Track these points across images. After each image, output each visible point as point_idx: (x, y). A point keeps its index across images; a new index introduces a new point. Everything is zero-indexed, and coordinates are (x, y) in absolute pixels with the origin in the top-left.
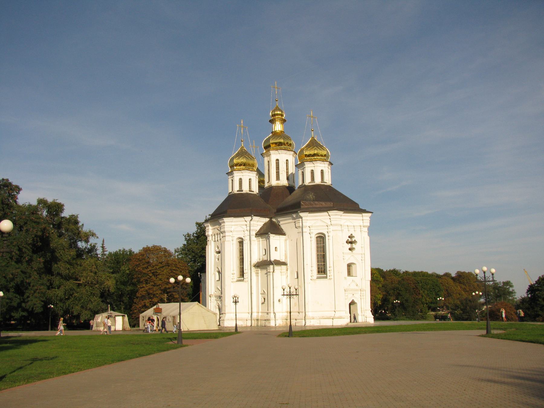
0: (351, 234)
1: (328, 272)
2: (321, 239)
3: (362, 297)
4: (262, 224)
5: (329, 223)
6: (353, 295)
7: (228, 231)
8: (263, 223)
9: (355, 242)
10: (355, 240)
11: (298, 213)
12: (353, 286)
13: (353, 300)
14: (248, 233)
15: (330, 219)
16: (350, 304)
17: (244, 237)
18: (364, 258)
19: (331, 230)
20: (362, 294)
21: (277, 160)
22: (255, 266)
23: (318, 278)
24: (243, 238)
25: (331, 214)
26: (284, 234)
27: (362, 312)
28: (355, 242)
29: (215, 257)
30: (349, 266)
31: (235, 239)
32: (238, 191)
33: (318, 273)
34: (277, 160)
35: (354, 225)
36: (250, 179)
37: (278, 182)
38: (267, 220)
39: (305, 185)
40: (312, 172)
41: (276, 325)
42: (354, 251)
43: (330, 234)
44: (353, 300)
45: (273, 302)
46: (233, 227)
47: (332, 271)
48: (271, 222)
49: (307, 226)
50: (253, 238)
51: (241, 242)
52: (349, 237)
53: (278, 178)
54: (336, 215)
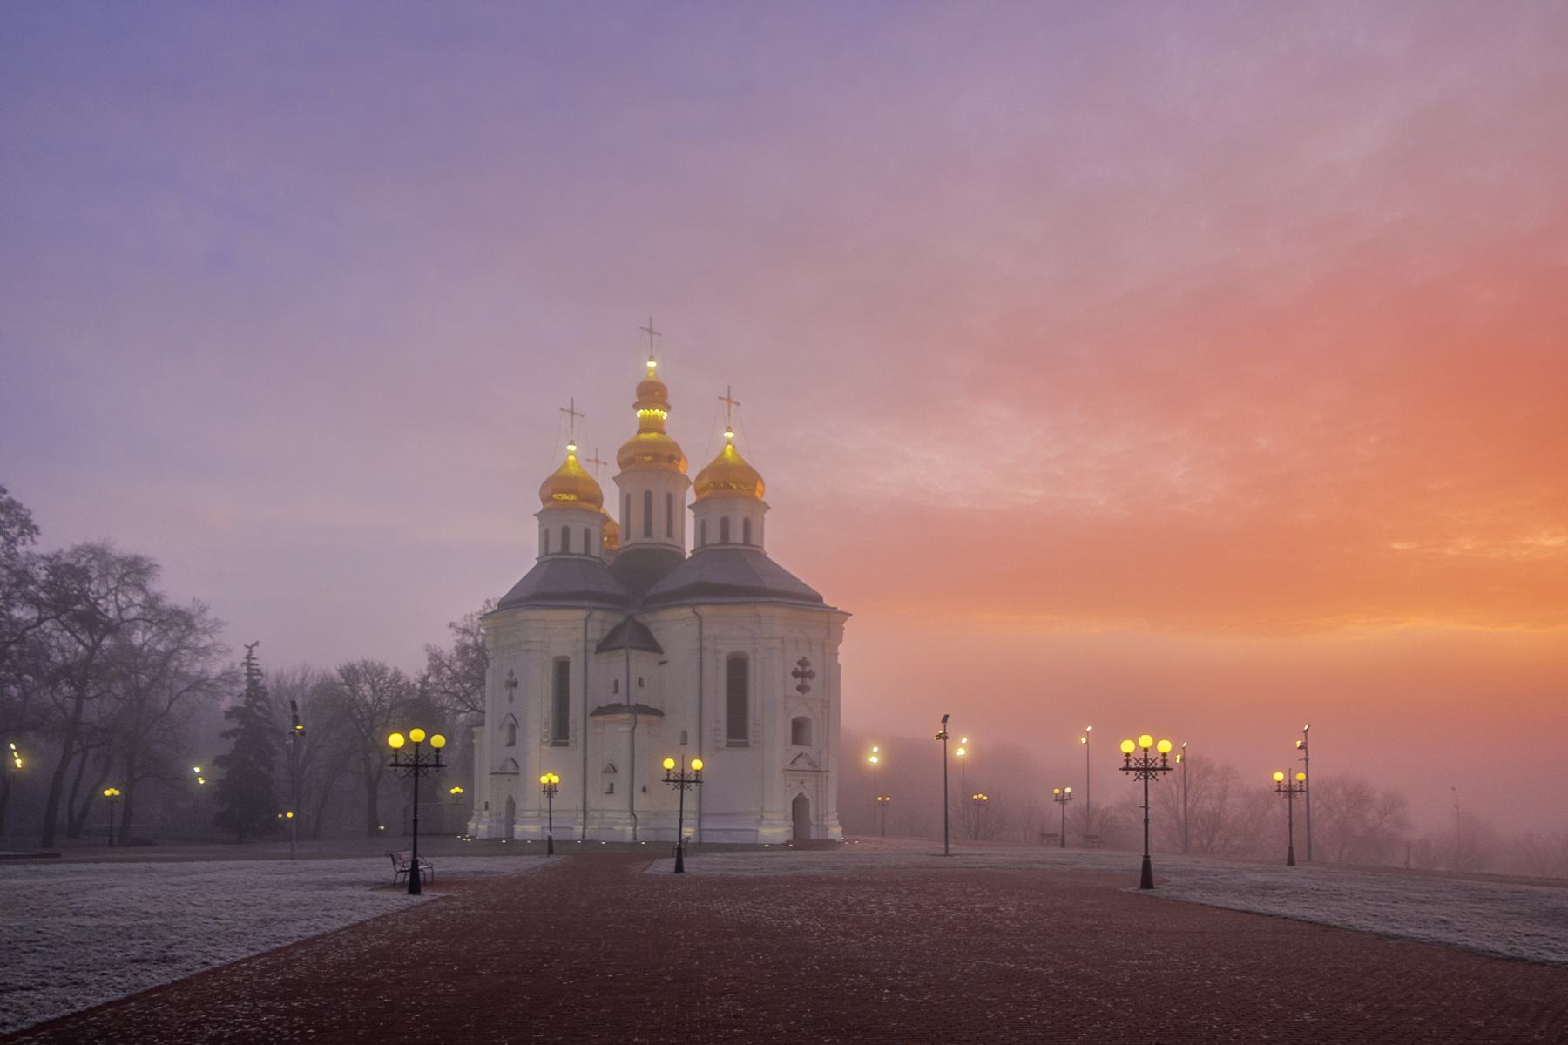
0: (804, 658)
4: (609, 628)
6: (802, 782)
9: (811, 675)
10: (810, 671)
13: (801, 794)
14: (580, 646)
22: (591, 715)
23: (729, 745)
28: (811, 675)
42: (807, 695)
44: (801, 794)
50: (592, 657)
51: (562, 668)
52: (799, 663)
53: (648, 531)
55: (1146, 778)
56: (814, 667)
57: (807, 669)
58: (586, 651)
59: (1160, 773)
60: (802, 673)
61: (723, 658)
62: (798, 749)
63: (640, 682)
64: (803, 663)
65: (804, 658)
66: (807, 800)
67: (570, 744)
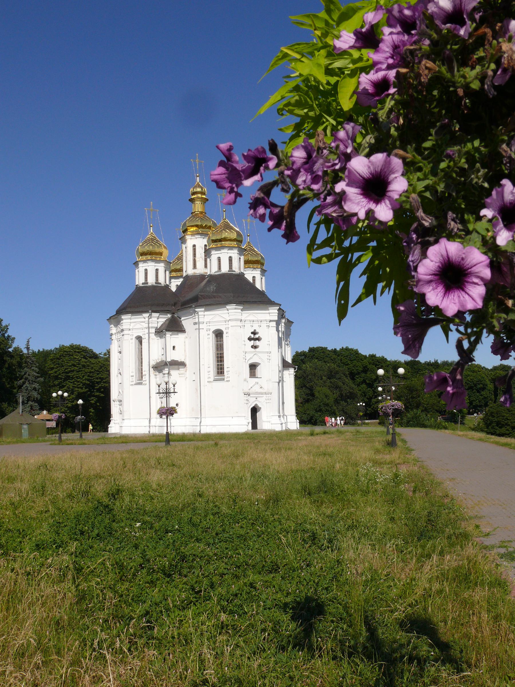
0: (255, 330)
7: (127, 329)
9: (259, 339)
10: (259, 337)
12: (257, 389)
13: (256, 404)
14: (147, 331)
21: (194, 246)
26: (183, 331)
29: (118, 357)
30: (253, 367)
31: (134, 337)
32: (143, 284)
33: (218, 373)
34: (194, 246)
36: (157, 270)
38: (169, 316)
39: (211, 275)
40: (219, 259)
44: (256, 404)
46: (132, 324)
48: (172, 317)
50: (153, 336)
52: (252, 333)
53: (195, 267)
54: (235, 309)
58: (149, 333)
59: (172, 394)
60: (254, 337)
61: (211, 333)
62: (254, 380)
64: (254, 333)
65: (255, 330)
66: (260, 408)
67: (144, 383)
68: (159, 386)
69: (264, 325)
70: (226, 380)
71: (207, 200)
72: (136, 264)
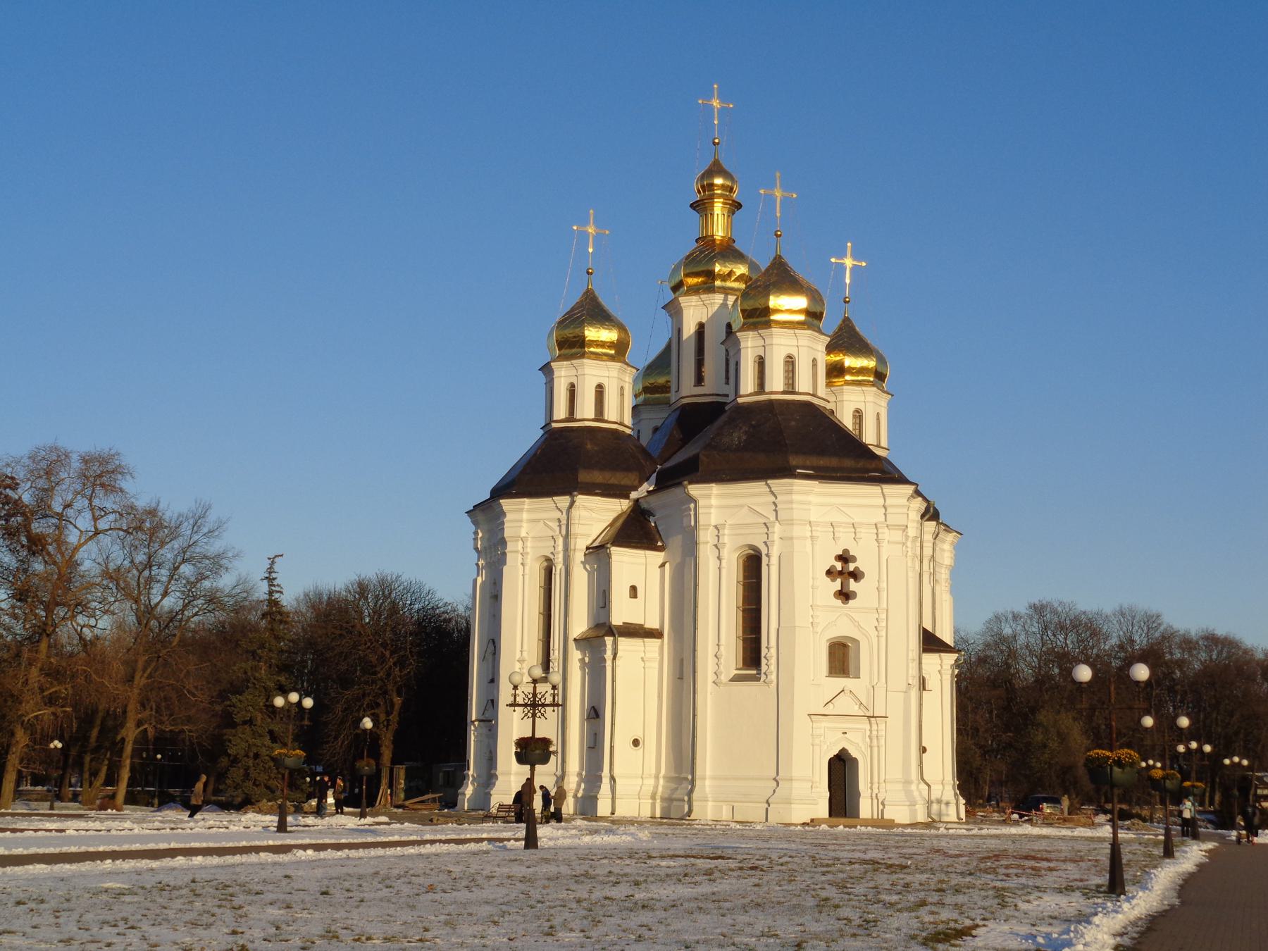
0: (846, 551)
1: (763, 661)
2: (753, 565)
3: (875, 741)
4: (610, 517)
5: (772, 518)
8: (615, 515)
9: (856, 575)
10: (857, 568)
11: (685, 487)
13: (843, 751)
15: (774, 503)
16: (831, 762)
17: (552, 553)
18: (884, 624)
19: (776, 537)
20: (874, 733)
23: (737, 679)
24: (552, 557)
25: (776, 489)
27: (871, 788)
28: (856, 575)
35: (856, 520)
37: (699, 390)
40: (761, 363)
41: (613, 813)
43: (775, 552)
45: (612, 747)
47: (773, 661)
49: (709, 525)
53: (699, 380)
55: (534, 716)
56: (859, 564)
57: (851, 567)
59: (549, 709)
62: (840, 682)
63: (634, 591)
64: (844, 558)
65: (846, 551)
66: (855, 761)
68: (515, 688)
69: (867, 535)
70: (763, 677)
71: (739, 206)
72: (547, 370)
